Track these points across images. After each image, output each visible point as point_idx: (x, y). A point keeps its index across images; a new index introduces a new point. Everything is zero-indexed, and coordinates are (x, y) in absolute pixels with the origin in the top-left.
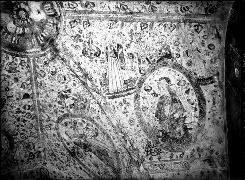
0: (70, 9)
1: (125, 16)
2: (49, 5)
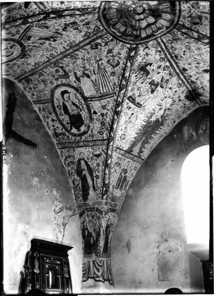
0: (105, 36)
1: (68, 52)
2: (122, 30)
